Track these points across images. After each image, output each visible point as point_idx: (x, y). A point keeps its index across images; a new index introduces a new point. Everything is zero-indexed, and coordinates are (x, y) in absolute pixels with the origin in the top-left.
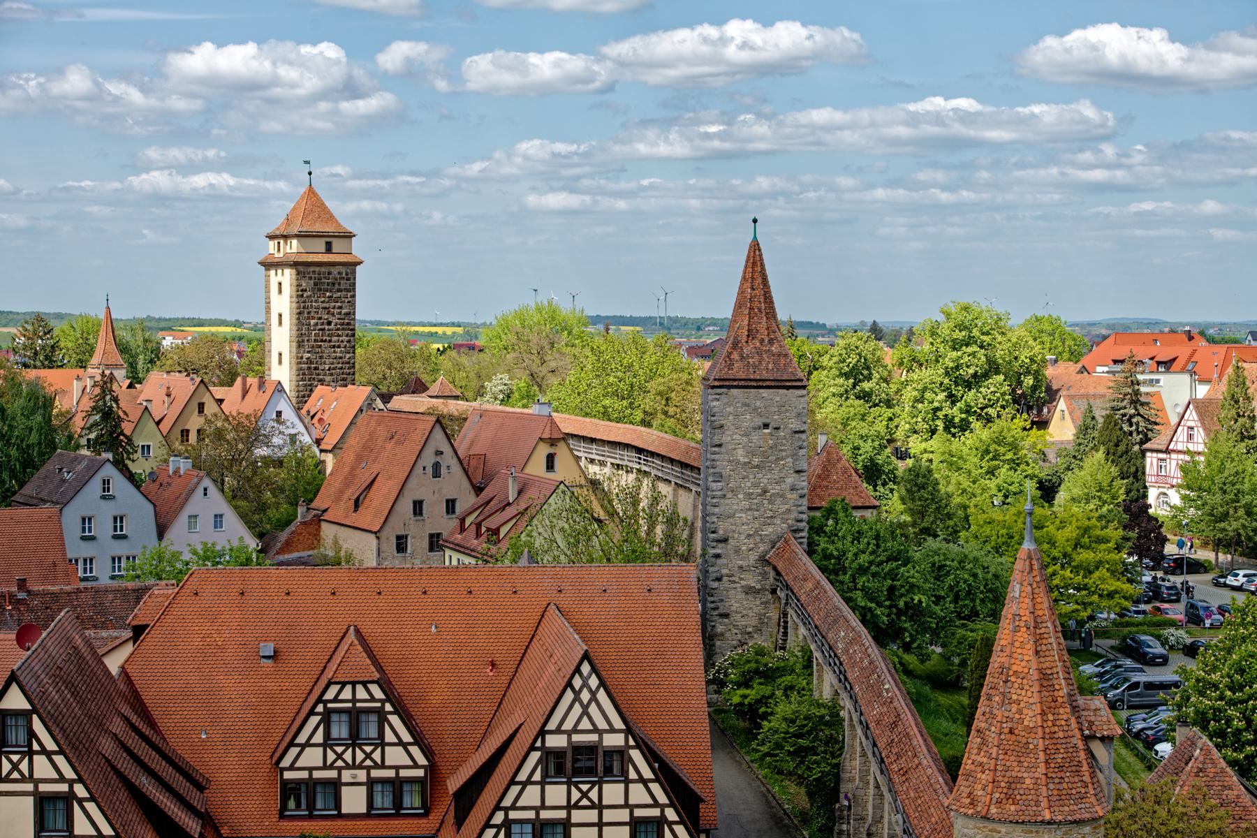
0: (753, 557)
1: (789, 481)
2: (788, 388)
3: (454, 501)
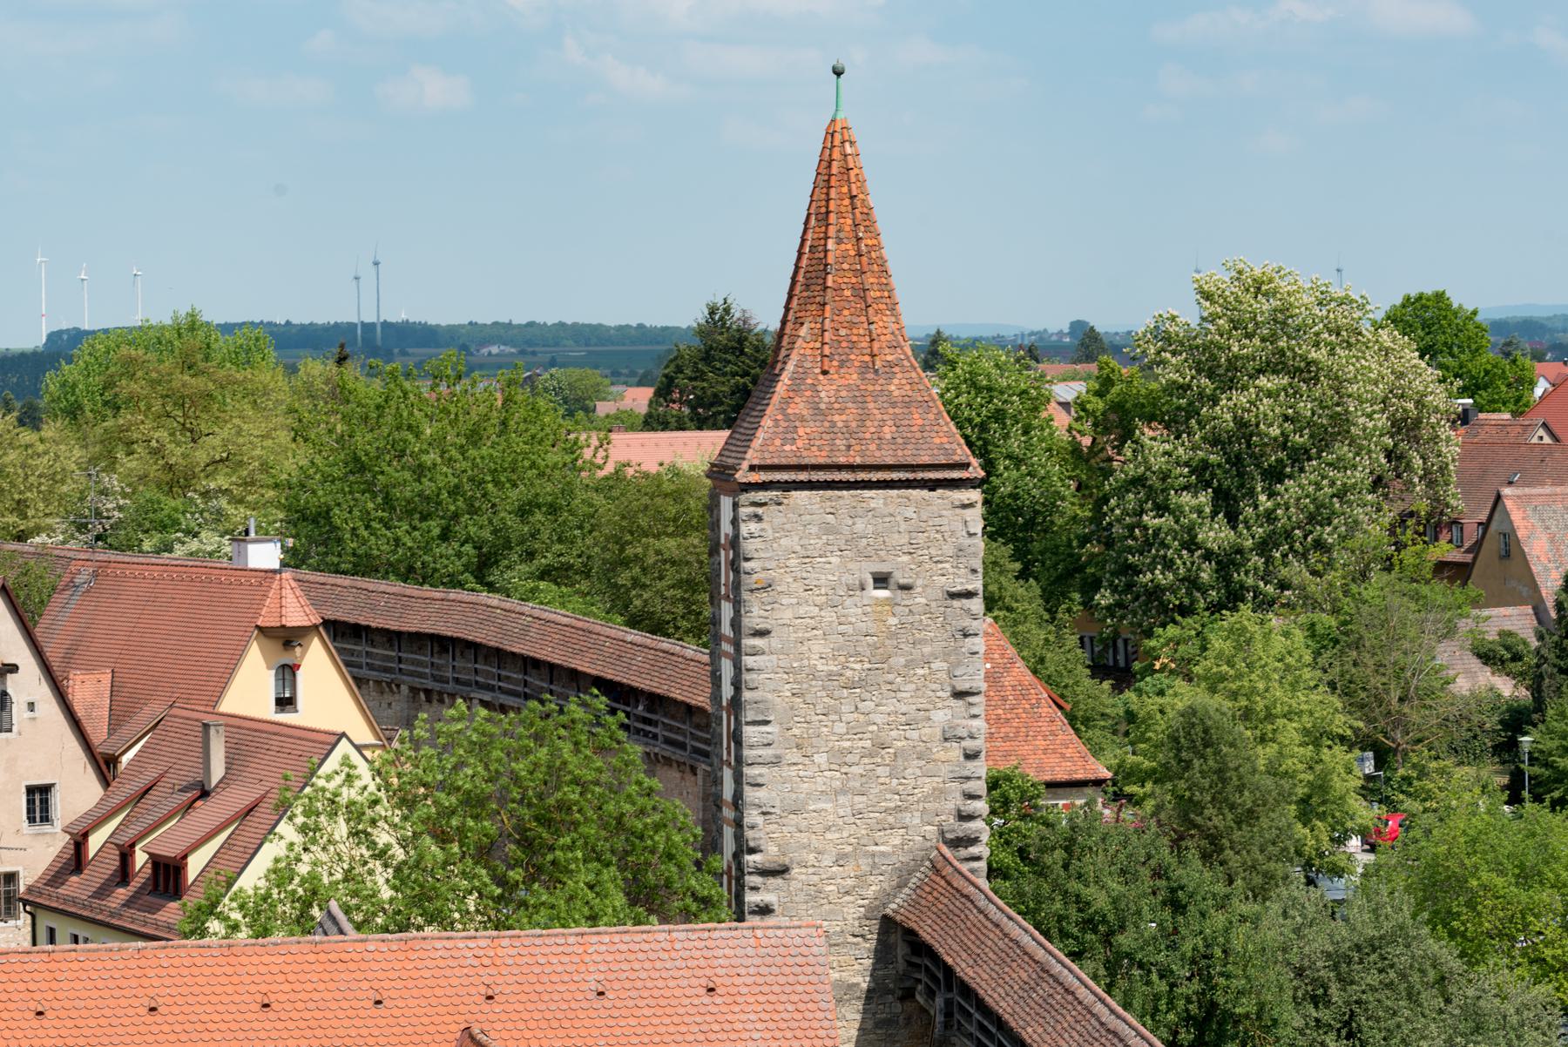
0: (852, 912)
1: (940, 717)
2: (933, 485)
3: (45, 790)
